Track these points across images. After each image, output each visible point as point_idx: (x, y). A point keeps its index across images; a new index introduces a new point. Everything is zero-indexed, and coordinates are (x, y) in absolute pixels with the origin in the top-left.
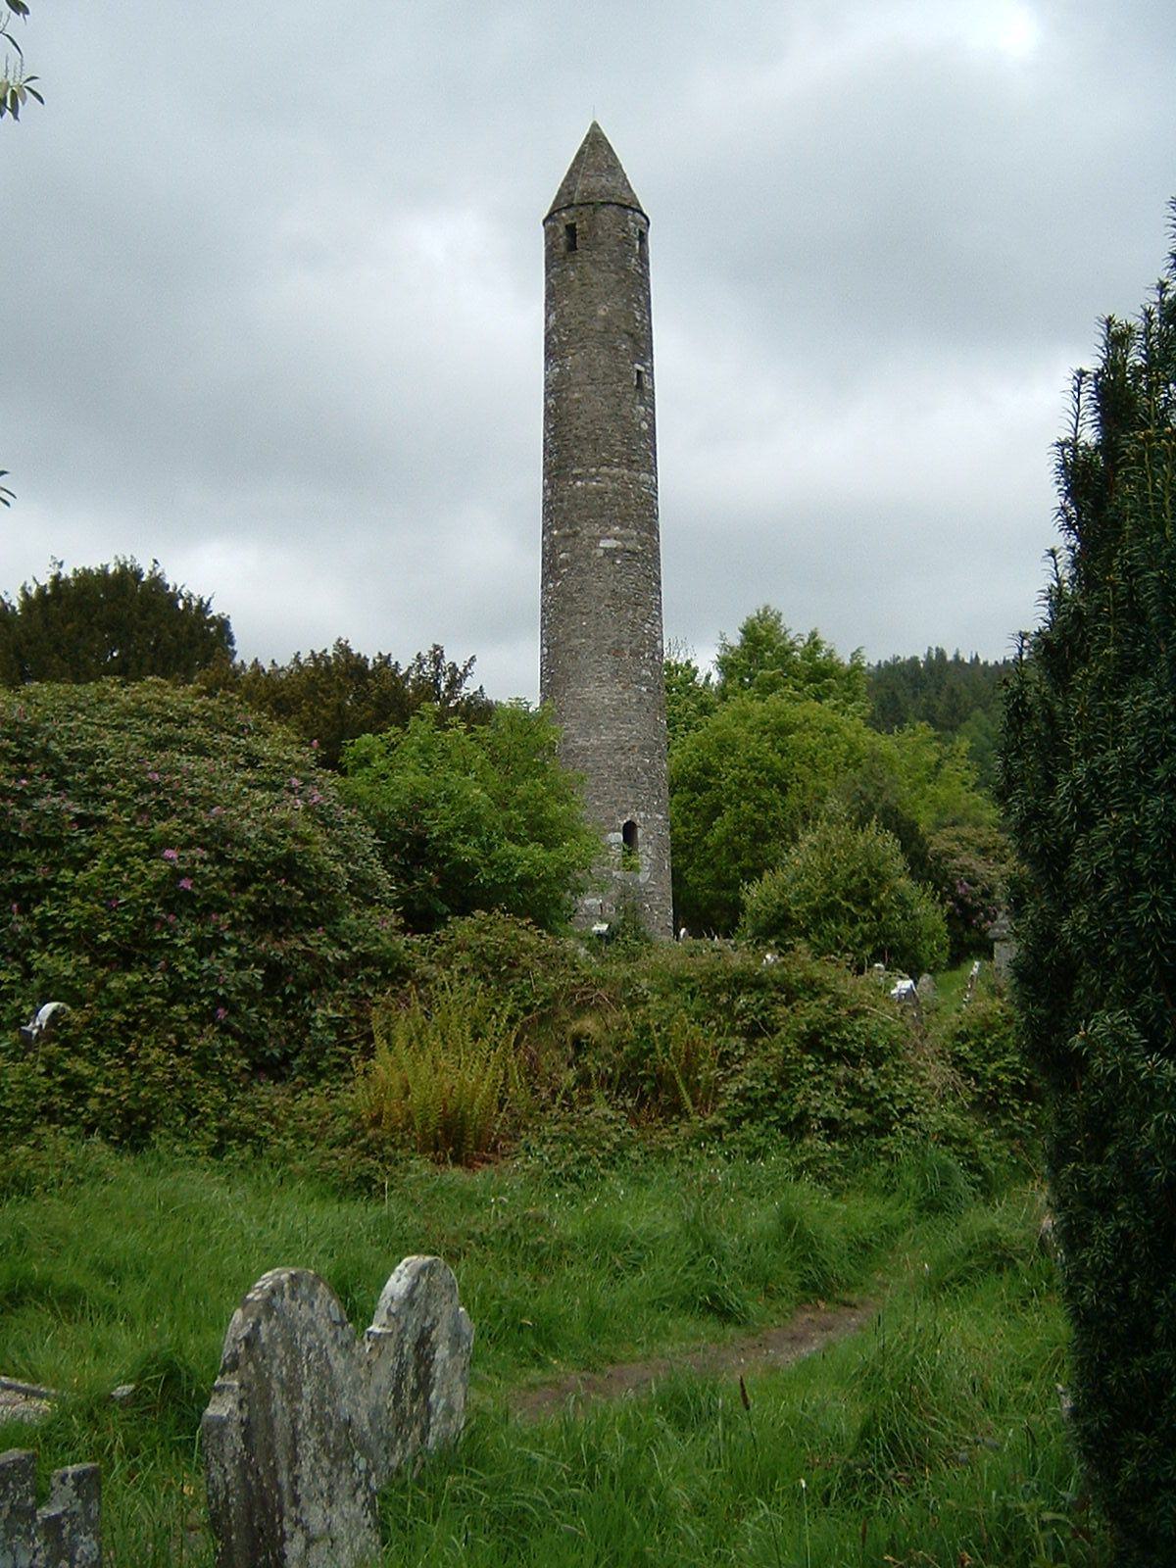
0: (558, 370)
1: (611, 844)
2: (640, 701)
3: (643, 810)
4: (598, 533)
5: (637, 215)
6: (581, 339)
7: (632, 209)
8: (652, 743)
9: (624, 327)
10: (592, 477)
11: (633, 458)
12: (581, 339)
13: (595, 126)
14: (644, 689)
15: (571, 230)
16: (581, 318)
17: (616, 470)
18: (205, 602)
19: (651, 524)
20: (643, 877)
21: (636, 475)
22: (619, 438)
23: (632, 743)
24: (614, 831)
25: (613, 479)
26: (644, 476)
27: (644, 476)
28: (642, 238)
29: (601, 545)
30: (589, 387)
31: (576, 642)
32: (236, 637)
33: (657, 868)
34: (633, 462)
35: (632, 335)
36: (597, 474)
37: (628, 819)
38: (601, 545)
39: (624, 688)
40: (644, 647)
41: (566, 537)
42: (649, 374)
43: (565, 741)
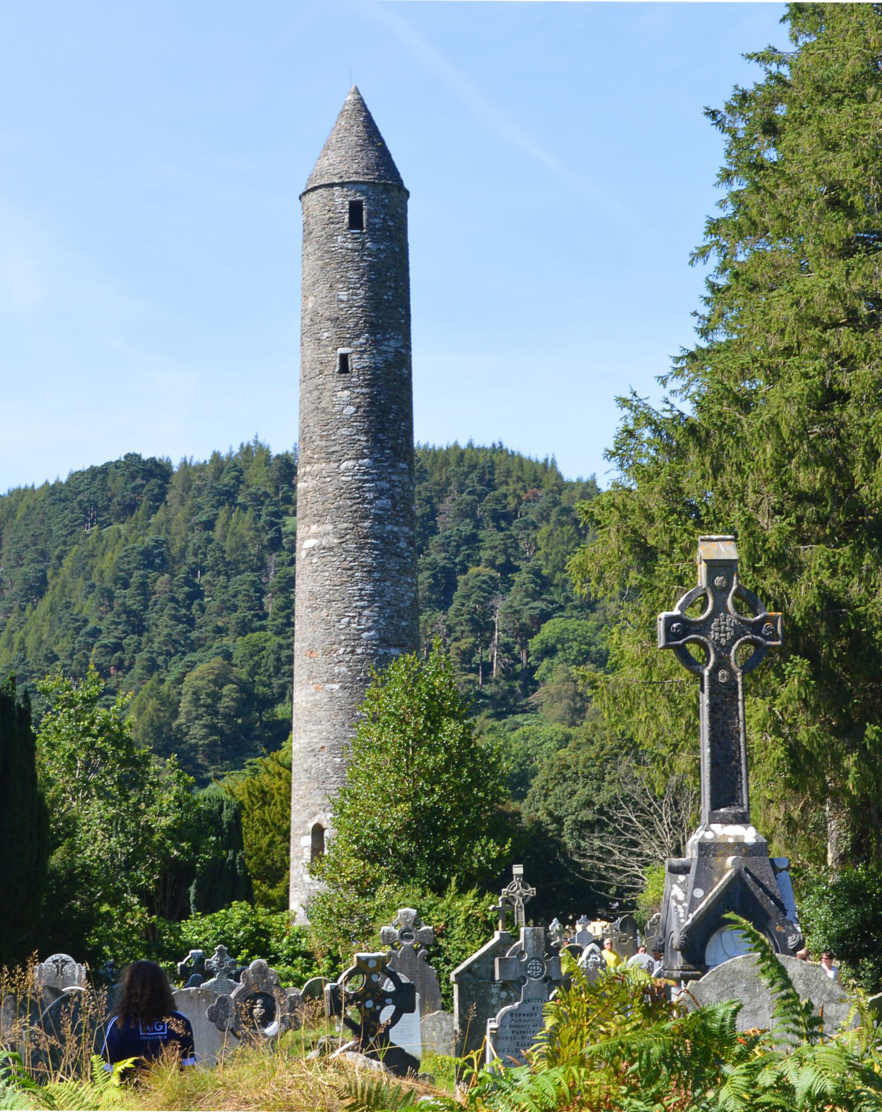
9: (327, 314)
11: (332, 449)
14: (336, 686)
23: (321, 745)
29: (304, 547)
34: (333, 452)
39: (316, 688)
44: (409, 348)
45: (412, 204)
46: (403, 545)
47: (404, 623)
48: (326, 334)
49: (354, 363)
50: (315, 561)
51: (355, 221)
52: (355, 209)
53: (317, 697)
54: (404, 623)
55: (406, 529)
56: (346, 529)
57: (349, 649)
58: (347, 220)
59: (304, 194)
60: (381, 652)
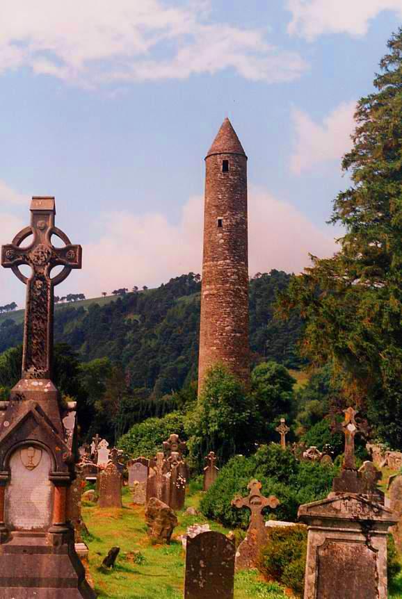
14: (215, 348)
22: (209, 249)
44: (246, 217)
45: (248, 162)
46: (242, 293)
47: (242, 324)
49: (224, 223)
51: (225, 169)
52: (225, 163)
54: (242, 324)
55: (244, 288)
59: (206, 158)
60: (233, 335)
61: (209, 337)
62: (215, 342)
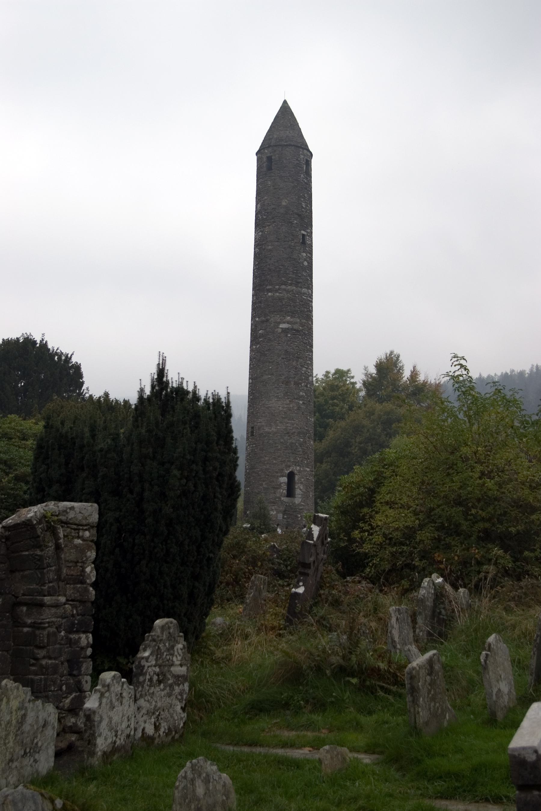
0: (261, 233)
1: (281, 483)
2: (299, 408)
3: (299, 466)
4: (279, 320)
5: (305, 151)
6: (273, 218)
7: (303, 148)
8: (305, 431)
9: (296, 211)
10: (277, 291)
12: (273, 218)
13: (285, 102)
14: (301, 402)
15: (269, 159)
16: (273, 206)
17: (289, 287)
18: (69, 356)
19: (307, 315)
20: (297, 500)
21: (300, 289)
22: (292, 270)
23: (294, 430)
24: (283, 476)
25: (288, 291)
26: (304, 290)
27: (304, 290)
28: (308, 164)
29: (280, 326)
30: (276, 243)
31: (265, 377)
32: (84, 375)
33: (305, 496)
34: (299, 283)
35: (299, 215)
36: (279, 289)
37: (290, 470)
38: (280, 326)
39: (290, 401)
40: (302, 380)
41: (263, 322)
42: (309, 236)
43: (259, 429)
48: (295, 221)
50: (289, 335)
53: (291, 406)
56: (305, 323)
57: (305, 384)
58: (305, 168)
61: (292, 385)
62: (301, 393)
